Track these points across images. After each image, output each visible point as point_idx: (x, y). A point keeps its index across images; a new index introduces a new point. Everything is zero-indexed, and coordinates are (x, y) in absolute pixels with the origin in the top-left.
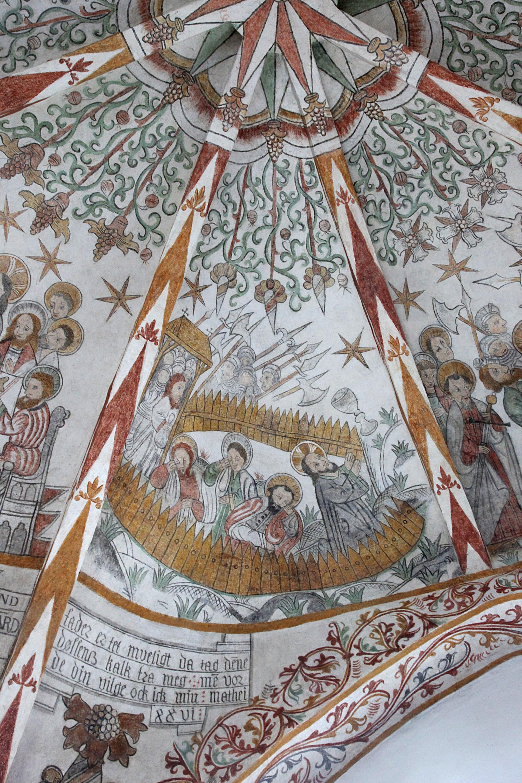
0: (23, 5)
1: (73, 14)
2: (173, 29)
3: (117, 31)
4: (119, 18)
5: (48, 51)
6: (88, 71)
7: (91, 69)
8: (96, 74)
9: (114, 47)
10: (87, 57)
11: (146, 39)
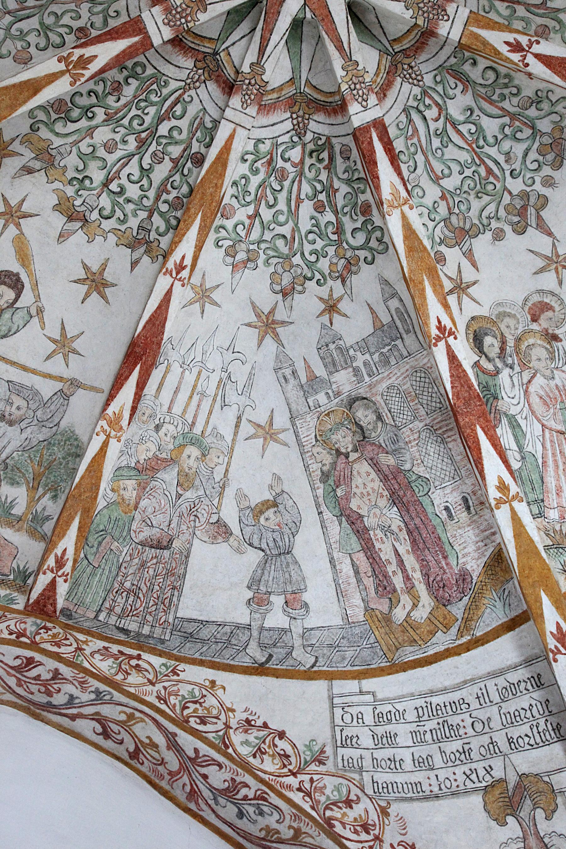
0: (502, 137)
1: (476, 95)
2: (417, 4)
3: (461, 47)
4: (446, 58)
5: (523, 87)
6: (515, 39)
7: (510, 37)
8: (511, 31)
9: (477, 37)
10: (504, 49)
11: (446, 18)
